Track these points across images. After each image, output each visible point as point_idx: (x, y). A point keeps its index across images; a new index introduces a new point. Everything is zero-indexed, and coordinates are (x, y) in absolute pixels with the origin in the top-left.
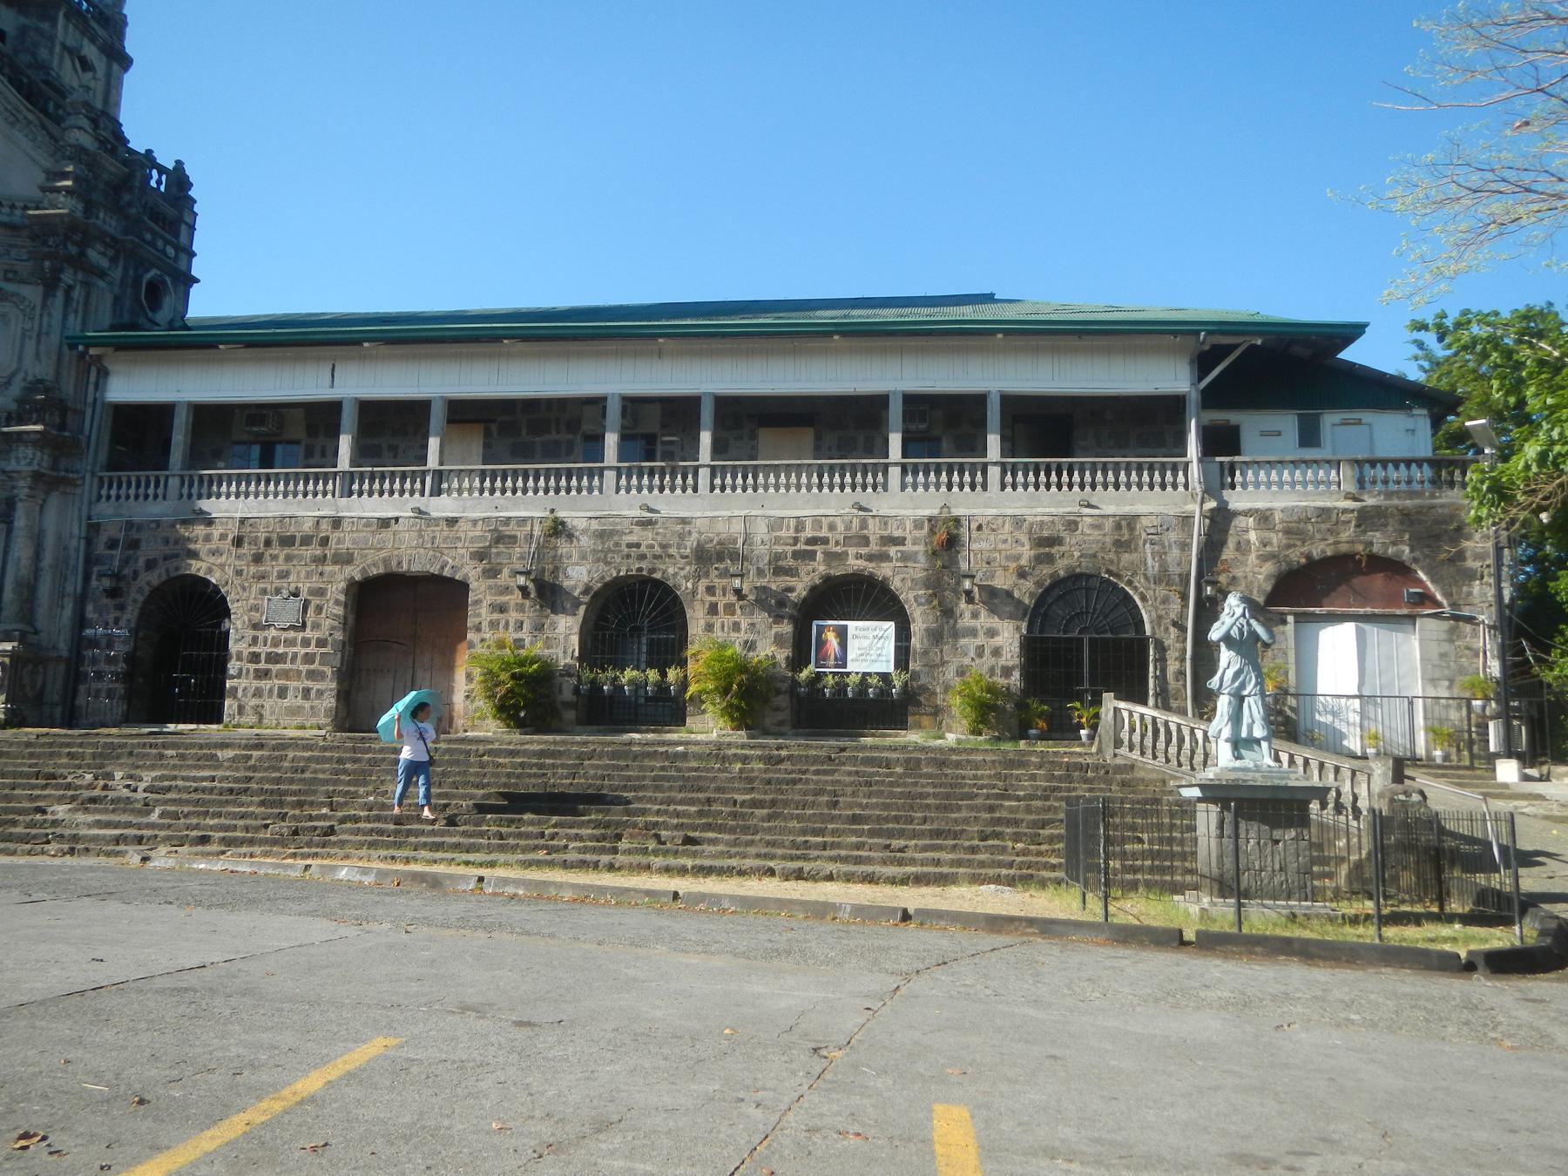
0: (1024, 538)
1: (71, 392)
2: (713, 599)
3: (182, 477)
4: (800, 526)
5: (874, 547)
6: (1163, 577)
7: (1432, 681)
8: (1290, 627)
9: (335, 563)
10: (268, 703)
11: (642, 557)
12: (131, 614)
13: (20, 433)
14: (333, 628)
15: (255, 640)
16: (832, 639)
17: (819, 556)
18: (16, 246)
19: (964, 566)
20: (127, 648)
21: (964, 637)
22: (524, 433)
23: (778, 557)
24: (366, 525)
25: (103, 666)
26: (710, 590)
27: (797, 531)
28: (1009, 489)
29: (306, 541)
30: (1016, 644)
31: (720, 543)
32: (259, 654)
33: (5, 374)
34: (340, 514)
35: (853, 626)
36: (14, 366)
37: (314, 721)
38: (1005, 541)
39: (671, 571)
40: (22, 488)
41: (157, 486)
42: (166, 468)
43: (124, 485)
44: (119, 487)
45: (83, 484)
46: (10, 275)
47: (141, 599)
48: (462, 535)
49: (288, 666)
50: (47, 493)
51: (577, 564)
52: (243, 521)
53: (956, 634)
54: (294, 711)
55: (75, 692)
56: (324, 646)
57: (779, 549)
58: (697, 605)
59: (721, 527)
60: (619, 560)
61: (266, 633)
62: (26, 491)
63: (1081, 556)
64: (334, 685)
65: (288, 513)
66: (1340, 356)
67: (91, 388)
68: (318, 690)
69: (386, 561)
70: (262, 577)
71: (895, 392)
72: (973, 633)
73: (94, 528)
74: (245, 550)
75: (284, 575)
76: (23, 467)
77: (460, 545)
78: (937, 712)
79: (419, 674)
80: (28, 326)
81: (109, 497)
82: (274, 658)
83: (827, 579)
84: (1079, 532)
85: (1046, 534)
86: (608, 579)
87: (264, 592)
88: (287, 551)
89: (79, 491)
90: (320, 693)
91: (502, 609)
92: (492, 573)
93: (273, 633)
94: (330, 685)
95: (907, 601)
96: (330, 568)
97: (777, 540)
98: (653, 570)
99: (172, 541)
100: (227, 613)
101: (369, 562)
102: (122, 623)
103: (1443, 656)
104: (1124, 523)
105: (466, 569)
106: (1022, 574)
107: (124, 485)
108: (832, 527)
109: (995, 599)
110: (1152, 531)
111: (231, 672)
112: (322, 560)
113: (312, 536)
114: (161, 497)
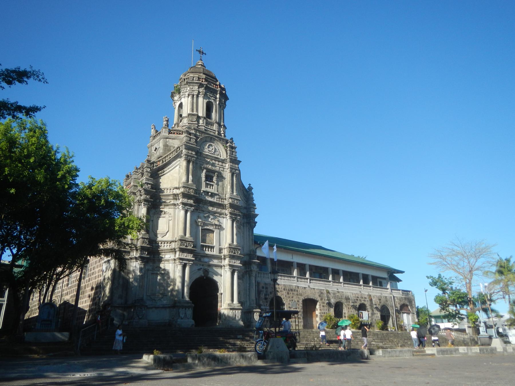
4: (355, 295)
5: (364, 299)
6: (391, 306)
7: (412, 322)
8: (402, 314)
9: (300, 295)
11: (339, 298)
12: (268, 304)
13: (255, 262)
14: (301, 309)
16: (361, 313)
19: (374, 303)
23: (354, 300)
24: (303, 288)
26: (348, 305)
27: (355, 295)
29: (295, 290)
35: (363, 312)
47: (270, 300)
52: (284, 285)
59: (347, 294)
64: (302, 320)
65: (290, 284)
66: (394, 274)
69: (307, 296)
70: (289, 297)
72: (375, 314)
75: (292, 297)
78: (374, 326)
91: (323, 306)
92: (321, 299)
100: (284, 304)
101: (305, 296)
102: (268, 305)
103: (413, 319)
105: (318, 298)
106: (379, 305)
109: (376, 308)
112: (297, 295)
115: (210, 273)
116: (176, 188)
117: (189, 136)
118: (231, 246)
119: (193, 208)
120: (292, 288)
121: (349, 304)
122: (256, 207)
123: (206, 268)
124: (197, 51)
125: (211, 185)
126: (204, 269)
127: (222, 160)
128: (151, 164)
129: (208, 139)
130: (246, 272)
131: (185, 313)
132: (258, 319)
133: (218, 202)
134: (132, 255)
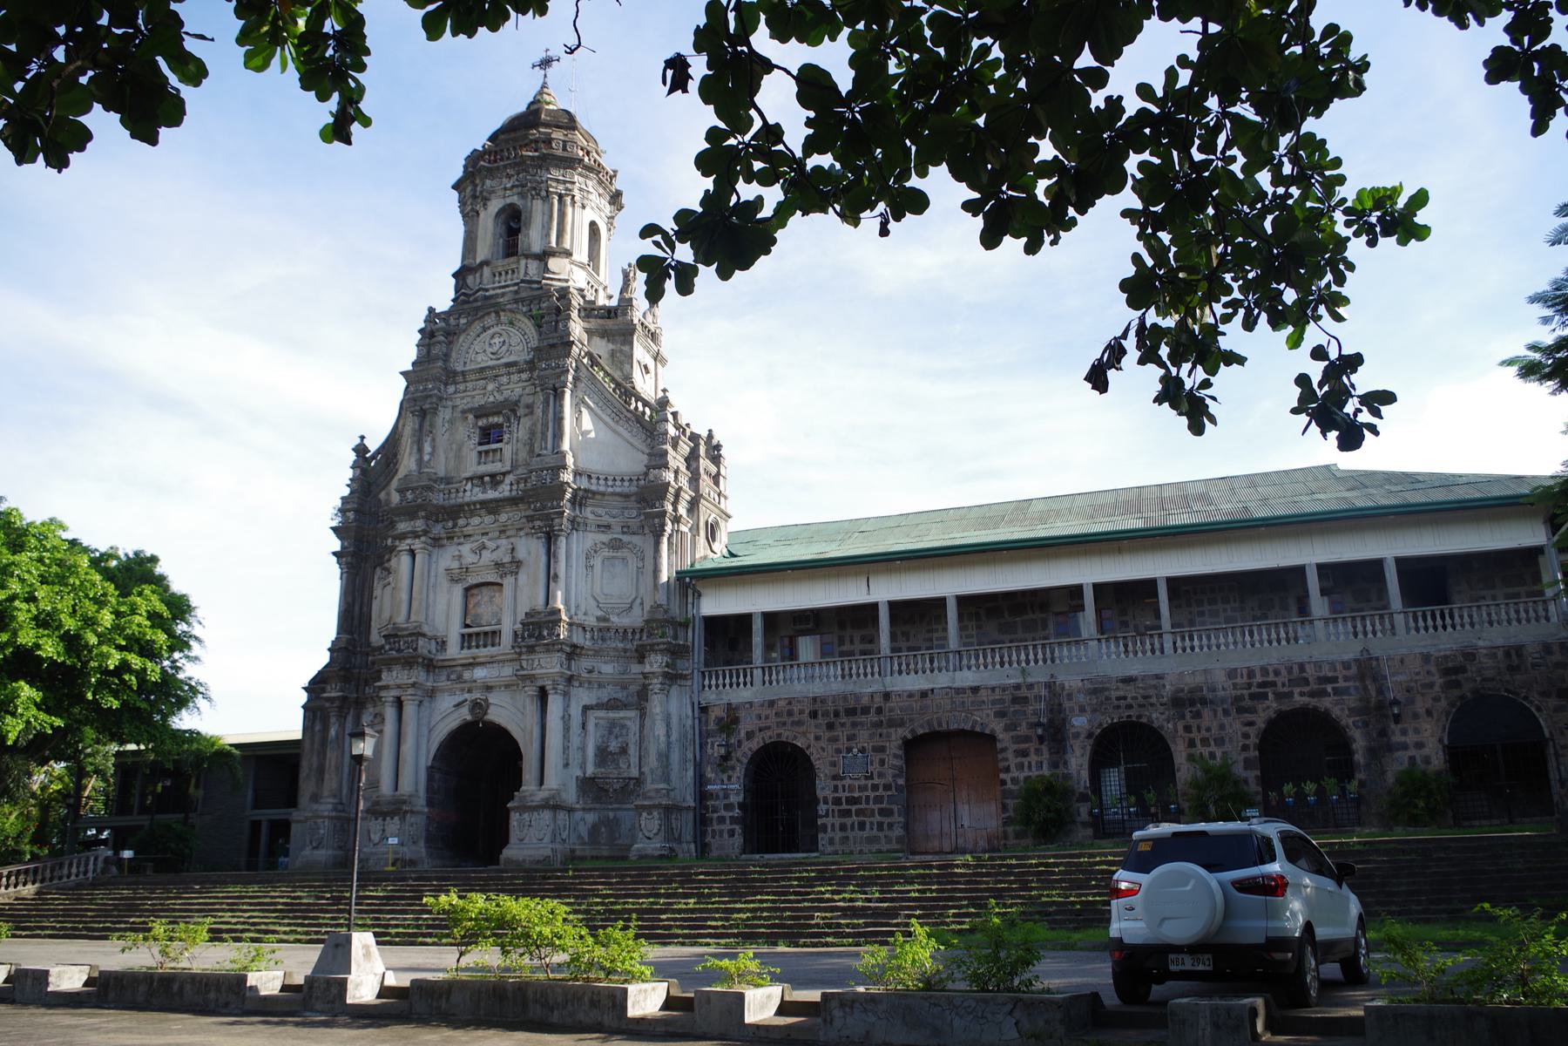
0: (1433, 669)
1: (678, 611)
2: (1192, 735)
3: (763, 668)
5: (1314, 686)
10: (851, 834)
11: (1129, 707)
12: (739, 772)
14: (895, 776)
15: (836, 789)
17: (1271, 696)
18: (627, 508)
20: (741, 798)
21: (1397, 750)
22: (1006, 615)
25: (723, 813)
26: (1188, 729)
28: (1413, 632)
29: (866, 710)
30: (1441, 753)
31: (1191, 691)
32: (840, 799)
33: (630, 601)
34: (888, 689)
36: (633, 597)
37: (889, 847)
38: (1418, 674)
39: (1154, 716)
40: (656, 684)
41: (745, 676)
42: (751, 663)
43: (721, 677)
44: (717, 679)
45: (693, 678)
46: (625, 530)
47: (745, 761)
48: (985, 699)
49: (863, 806)
50: (670, 686)
51: (1078, 716)
52: (815, 699)
53: (1391, 748)
54: (871, 840)
55: (703, 834)
56: (890, 789)
57: (1239, 692)
58: (1180, 741)
59: (1188, 679)
60: (1111, 710)
61: (844, 782)
62: (659, 686)
63: (1484, 680)
67: (690, 606)
68: (889, 823)
69: (928, 721)
70: (834, 740)
71: (1310, 565)
72: (1405, 747)
73: (704, 710)
74: (820, 720)
76: (656, 668)
77: (984, 707)
79: (960, 807)
80: (640, 565)
81: (710, 687)
82: (852, 801)
83: (1282, 716)
84: (1477, 661)
85: (1450, 665)
86: (1105, 726)
87: (838, 751)
88: (852, 719)
89: (689, 683)
90: (891, 826)
91: (1024, 754)
93: (847, 782)
94: (897, 818)
95: (1348, 726)
96: (885, 731)
97: (1235, 685)
98: (1139, 717)
99: (763, 718)
104: (1513, 652)
107: (721, 677)
108: (1277, 673)
110: (1536, 655)
111: (820, 812)
112: (879, 724)
113: (869, 707)
114: (749, 684)
118: (532, 616)
119: (423, 539)
120: (852, 704)
121: (1194, 723)
123: (478, 696)
124: (534, 66)
125: (494, 451)
126: (472, 701)
127: (526, 362)
128: (373, 457)
131: (384, 830)
132: (655, 831)
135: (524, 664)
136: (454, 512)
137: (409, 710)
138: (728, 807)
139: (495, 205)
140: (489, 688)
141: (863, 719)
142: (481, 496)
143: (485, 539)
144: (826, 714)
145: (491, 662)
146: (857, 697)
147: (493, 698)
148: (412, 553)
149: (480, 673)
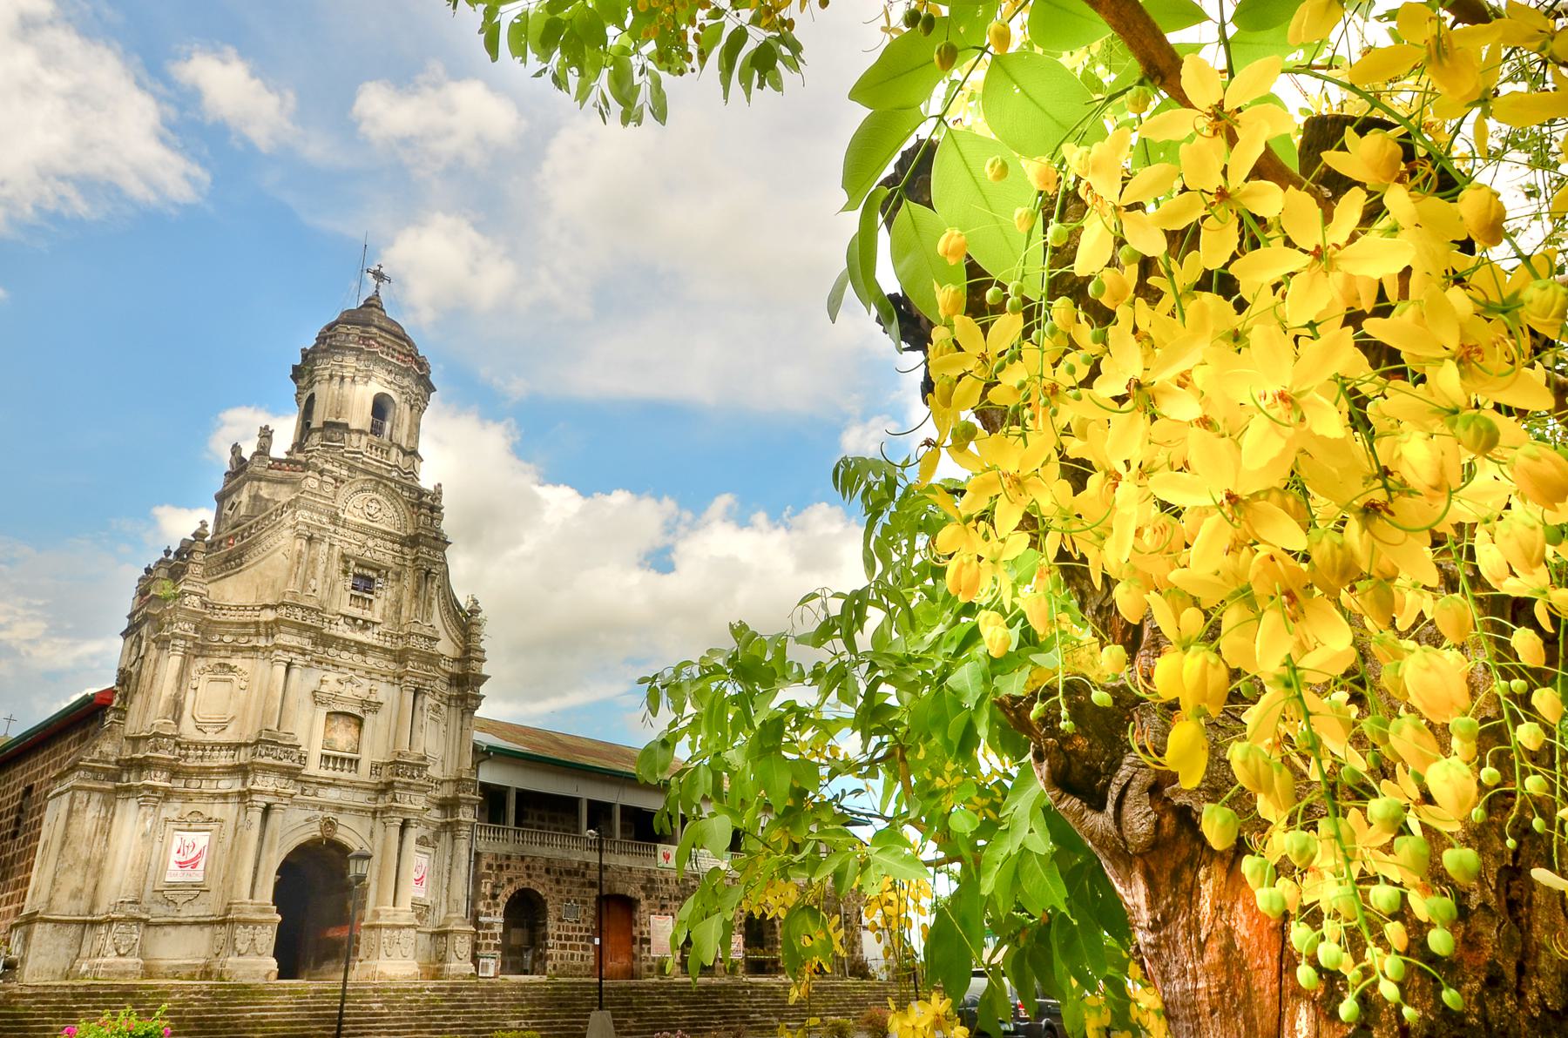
12: (501, 909)
52: (548, 859)
70: (559, 892)
73: (478, 855)
82: (568, 938)
87: (562, 900)
93: (565, 924)
112: (583, 885)
115: (340, 829)
116: (265, 607)
117: (318, 476)
120: (569, 867)
122: (486, 656)
123: (331, 815)
125: (364, 599)
126: (324, 819)
129: (369, 486)
130: (445, 826)
133: (381, 644)
134: (125, 779)
135: (398, 796)
136: (325, 640)
137: (275, 818)
138: (494, 936)
139: (375, 387)
140: (340, 809)
141: (575, 879)
142: (350, 635)
143: (351, 674)
144: (555, 872)
145: (352, 786)
146: (571, 862)
147: (342, 819)
148: (289, 666)
149: (331, 795)
